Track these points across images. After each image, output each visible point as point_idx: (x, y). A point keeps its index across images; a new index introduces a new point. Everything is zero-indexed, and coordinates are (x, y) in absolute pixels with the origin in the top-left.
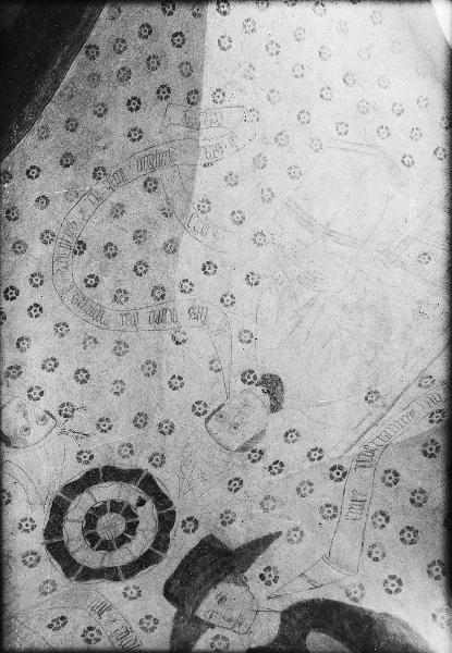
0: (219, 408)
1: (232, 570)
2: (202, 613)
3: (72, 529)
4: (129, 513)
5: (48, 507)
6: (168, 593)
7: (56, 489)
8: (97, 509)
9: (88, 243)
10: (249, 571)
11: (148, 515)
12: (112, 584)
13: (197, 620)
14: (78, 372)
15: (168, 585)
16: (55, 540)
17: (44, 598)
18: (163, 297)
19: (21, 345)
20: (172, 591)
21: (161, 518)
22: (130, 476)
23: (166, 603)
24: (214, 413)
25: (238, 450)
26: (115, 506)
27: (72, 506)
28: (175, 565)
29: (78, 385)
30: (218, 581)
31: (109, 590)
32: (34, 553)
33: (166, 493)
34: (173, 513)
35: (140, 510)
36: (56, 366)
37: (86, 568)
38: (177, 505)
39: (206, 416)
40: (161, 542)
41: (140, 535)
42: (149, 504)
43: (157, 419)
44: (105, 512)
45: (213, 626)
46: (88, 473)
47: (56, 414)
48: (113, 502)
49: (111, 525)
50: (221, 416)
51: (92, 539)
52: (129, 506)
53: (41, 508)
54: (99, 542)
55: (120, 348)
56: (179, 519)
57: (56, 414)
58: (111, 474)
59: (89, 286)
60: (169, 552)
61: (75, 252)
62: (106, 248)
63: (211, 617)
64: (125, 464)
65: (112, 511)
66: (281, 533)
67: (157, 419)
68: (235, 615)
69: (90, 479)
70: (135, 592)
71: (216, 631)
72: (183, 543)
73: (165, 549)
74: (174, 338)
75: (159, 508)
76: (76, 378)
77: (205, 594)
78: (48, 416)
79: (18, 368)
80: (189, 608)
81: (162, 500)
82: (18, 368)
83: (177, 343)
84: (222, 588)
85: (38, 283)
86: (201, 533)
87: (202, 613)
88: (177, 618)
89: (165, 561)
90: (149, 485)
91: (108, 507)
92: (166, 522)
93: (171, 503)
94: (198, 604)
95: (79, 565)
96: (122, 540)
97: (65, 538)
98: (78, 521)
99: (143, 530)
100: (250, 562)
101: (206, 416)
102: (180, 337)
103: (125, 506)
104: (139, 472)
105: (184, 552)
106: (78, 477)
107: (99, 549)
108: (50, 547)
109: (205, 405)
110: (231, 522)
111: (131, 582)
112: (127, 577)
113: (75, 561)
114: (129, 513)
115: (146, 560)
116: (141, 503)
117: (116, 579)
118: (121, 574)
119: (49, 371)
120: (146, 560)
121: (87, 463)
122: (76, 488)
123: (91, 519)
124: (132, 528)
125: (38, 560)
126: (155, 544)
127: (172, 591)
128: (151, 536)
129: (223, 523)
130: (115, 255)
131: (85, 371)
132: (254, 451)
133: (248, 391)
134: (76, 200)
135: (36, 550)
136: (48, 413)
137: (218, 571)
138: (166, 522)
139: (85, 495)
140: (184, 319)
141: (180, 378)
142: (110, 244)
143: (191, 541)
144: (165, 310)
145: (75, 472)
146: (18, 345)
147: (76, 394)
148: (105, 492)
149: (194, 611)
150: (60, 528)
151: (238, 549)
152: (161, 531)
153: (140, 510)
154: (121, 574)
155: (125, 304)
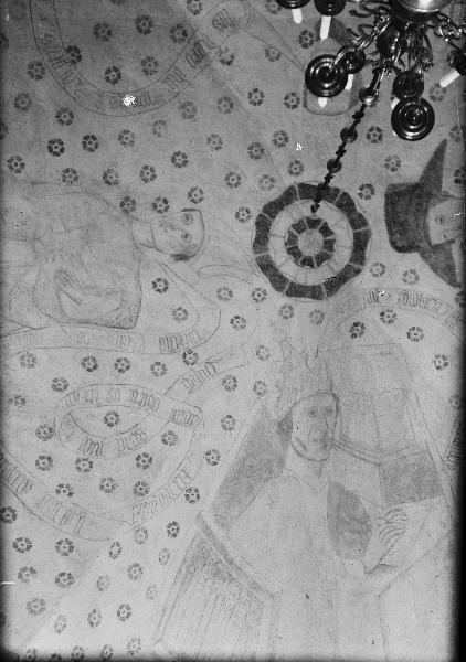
1: (429, 195)
3: (290, 269)
7: (252, 256)
8: (289, 240)
9: (76, 42)
10: (443, 185)
12: (360, 276)
13: (437, 248)
15: (393, 243)
16: (287, 287)
17: (324, 324)
18: (185, 34)
19: (111, 180)
20: (399, 244)
21: (340, 206)
22: (288, 197)
23: (407, 255)
26: (299, 227)
27: (272, 255)
28: (383, 227)
29: (184, 169)
30: (426, 211)
31: (364, 282)
32: (284, 307)
34: (345, 194)
35: (319, 214)
36: (152, 170)
39: (301, 101)
40: (357, 222)
41: (336, 230)
43: (267, 139)
44: (296, 237)
46: (257, 224)
47: (193, 206)
48: (294, 226)
49: (310, 243)
52: (308, 219)
53: (254, 276)
54: (314, 261)
55: (188, 110)
56: (354, 194)
57: (193, 206)
58: (273, 208)
59: (115, 82)
60: (370, 223)
61: (73, 62)
62: (96, 33)
64: (274, 194)
66: (445, 141)
67: (267, 139)
70: (379, 268)
72: (373, 209)
73: (365, 223)
74: (223, 61)
77: (426, 228)
79: (127, 199)
82: (127, 199)
83: (229, 63)
85: (68, 118)
86: (381, 191)
89: (373, 231)
91: (295, 233)
92: (346, 205)
94: (427, 236)
95: (319, 286)
96: (329, 245)
97: (291, 279)
98: (287, 260)
99: (336, 225)
100: (439, 178)
101: (301, 101)
102: (227, 57)
104: (291, 188)
106: (255, 233)
108: (289, 294)
109: (293, 94)
110: (398, 164)
111: (369, 264)
113: (313, 287)
114: (313, 223)
115: (360, 244)
117: (358, 272)
118: (356, 266)
119: (152, 179)
120: (360, 244)
121: (249, 217)
123: (294, 251)
124: (326, 230)
125: (291, 308)
126: (353, 224)
128: (345, 223)
129: (393, 170)
130: (110, 33)
131: (177, 154)
133: (433, 98)
134: (28, 12)
136: (185, 210)
137: (420, 204)
139: (272, 240)
140: (217, 38)
141: (256, 90)
142: (97, 27)
144: (197, 44)
145: (248, 232)
146: (107, 182)
147: (163, 167)
148: (282, 224)
149: (429, 244)
150: (281, 276)
151: (422, 178)
152: (349, 215)
153: (319, 214)
154: (356, 266)
155: (159, 69)
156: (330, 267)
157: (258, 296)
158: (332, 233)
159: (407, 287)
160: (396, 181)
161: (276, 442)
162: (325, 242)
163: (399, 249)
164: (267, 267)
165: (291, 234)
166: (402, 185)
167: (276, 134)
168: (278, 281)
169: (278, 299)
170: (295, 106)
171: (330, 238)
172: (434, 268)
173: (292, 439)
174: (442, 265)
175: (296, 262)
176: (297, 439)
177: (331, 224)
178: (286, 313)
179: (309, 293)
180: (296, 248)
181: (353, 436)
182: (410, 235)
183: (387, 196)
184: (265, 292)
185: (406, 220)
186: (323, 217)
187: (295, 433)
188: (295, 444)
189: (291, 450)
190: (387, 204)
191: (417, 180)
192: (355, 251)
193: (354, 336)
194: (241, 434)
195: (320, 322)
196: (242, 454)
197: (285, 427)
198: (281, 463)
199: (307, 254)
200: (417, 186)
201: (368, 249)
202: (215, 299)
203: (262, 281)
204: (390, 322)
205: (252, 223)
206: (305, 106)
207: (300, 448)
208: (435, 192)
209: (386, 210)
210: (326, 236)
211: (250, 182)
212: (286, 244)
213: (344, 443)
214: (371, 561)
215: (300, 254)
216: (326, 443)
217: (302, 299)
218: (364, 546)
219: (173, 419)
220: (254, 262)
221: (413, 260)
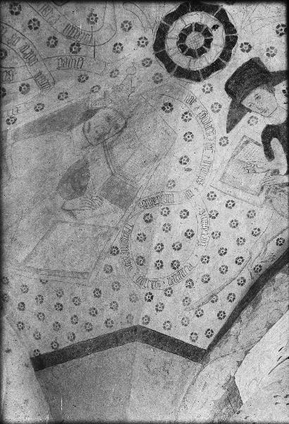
1: (267, 82)
2: (246, 103)
3: (171, 44)
4: (207, 33)
5: (155, 30)
6: (229, 89)
11: (219, 37)
15: (228, 83)
20: (229, 86)
21: (227, 39)
26: (198, 27)
27: (171, 29)
30: (257, 86)
31: (196, 88)
33: (233, 23)
34: (236, 37)
37: (179, 67)
38: (239, 33)
40: (226, 55)
41: (213, 48)
42: (221, 29)
44: (192, 31)
45: (250, 111)
48: (196, 24)
49: (194, 41)
51: (183, 48)
52: (207, 28)
56: (239, 42)
63: (250, 106)
68: (264, 107)
71: (252, 114)
72: (240, 58)
73: (228, 60)
77: (248, 93)
80: (239, 99)
84: (258, 91)
86: (252, 54)
87: (246, 103)
92: (231, 42)
94: (244, 97)
103: (205, 28)
105: (240, 64)
107: (187, 55)
111: (206, 81)
112: (205, 78)
113: (172, 62)
114: (207, 33)
115: (217, 66)
116: (215, 27)
117: (199, 80)
120: (217, 66)
123: (183, 37)
125: (151, 62)
127: (229, 86)
128: (220, 50)
129: (268, 55)
137: (259, 80)
138: (231, 42)
139: (179, 21)
151: (274, 72)
153: (214, 32)
156: (190, 61)
157: (142, 42)
158: (209, 47)
159: (210, 110)
160: (263, 60)
161: (77, 118)
162: (202, 48)
163: (227, 89)
165: (191, 26)
166: (263, 64)
168: (159, 45)
169: (149, 52)
171: (206, 49)
173: (87, 122)
175: (177, 43)
176: (90, 124)
177: (214, 42)
178: (146, 63)
179: (167, 63)
181: (116, 150)
184: (147, 43)
186: (214, 35)
187: (92, 120)
189: (83, 124)
191: (271, 71)
192: (208, 67)
193: (163, 108)
194: (63, 104)
195: (157, 82)
196: (56, 113)
197: (90, 113)
198: (71, 128)
199: (187, 44)
200: (267, 72)
201: (215, 73)
202: (119, 25)
203: (151, 37)
204: (185, 120)
207: (86, 128)
208: (270, 84)
209: (243, 65)
210: (205, 45)
213: (108, 148)
214: (68, 206)
215: (184, 41)
216: (100, 138)
217: (161, 63)
218: (72, 197)
220: (158, 25)
221: (226, 101)
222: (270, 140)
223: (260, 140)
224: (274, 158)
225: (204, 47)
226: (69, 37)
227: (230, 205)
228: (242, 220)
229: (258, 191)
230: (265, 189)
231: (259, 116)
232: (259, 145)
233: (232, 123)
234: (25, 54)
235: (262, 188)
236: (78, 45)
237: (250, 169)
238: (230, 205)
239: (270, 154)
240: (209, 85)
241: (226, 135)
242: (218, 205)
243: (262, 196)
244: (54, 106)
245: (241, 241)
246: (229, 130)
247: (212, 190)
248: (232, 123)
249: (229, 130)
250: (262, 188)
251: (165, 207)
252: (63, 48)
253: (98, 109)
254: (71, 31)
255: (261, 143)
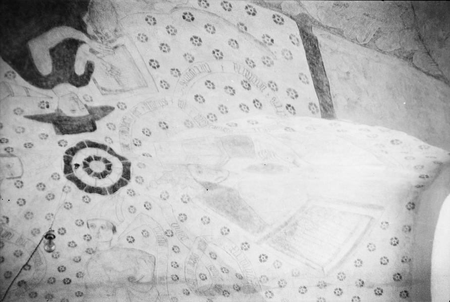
0: (10, 178)
1: (59, 117)
4: (86, 165)
5: (117, 193)
6: (94, 128)
14: (63, 234)
16: (124, 179)
20: (92, 128)
21: (73, 154)
24: (13, 178)
25: (15, 156)
26: (90, 172)
29: (66, 229)
32: (137, 181)
34: (66, 153)
35: (80, 162)
39: (18, 179)
40: (82, 146)
42: (74, 162)
45: (86, 106)
47: (85, 224)
50: (12, 175)
51: (109, 167)
53: (120, 194)
57: (85, 224)
58: (80, 185)
64: (73, 186)
65: (92, 171)
69: (91, 190)
72: (72, 140)
75: (71, 159)
76: (65, 232)
78: (89, 226)
80: (90, 118)
81: (67, 161)
84: (70, 114)
86: (61, 137)
88: (98, 119)
90: (68, 169)
92: (73, 151)
93: (64, 157)
94: (88, 116)
100: (47, 116)
103: (85, 169)
107: (109, 162)
109: (15, 184)
113: (123, 165)
114: (86, 165)
116: (77, 165)
118: (108, 149)
121: (88, 197)
122: (100, 191)
123: (103, 175)
124: (89, 159)
132: (9, 152)
135: (135, 182)
136: (88, 227)
137: (66, 120)
143: (67, 137)
145: (95, 197)
146: (80, 260)
150: (119, 182)
151: (49, 122)
153: (80, 162)
154: (108, 149)
160: (54, 133)
161: (216, 192)
164: (114, 189)
166: (55, 129)
167: (39, 189)
169: (132, 184)
170: (22, 182)
172: (104, 115)
173: (216, 182)
174: (101, 112)
175: (110, 174)
176: (216, 180)
179: (127, 167)
180: (101, 174)
182: (85, 123)
183: (63, 134)
184: (129, 190)
185: (77, 125)
188: (219, 181)
190: (68, 134)
194: (211, 213)
197: (208, 187)
198: (230, 190)
203: (122, 191)
205: (91, 195)
206: (20, 177)
208: (57, 115)
209: (71, 134)
210: (92, 160)
211: (69, 198)
212: (100, 179)
219: (203, 251)
220: (113, 195)
222: (82, 76)
223: (91, 82)
224: (88, 62)
225: (94, 159)
226: (166, 241)
227: (154, 64)
228: (155, 44)
229: (120, 49)
230: (114, 44)
231: (81, 98)
232: (94, 80)
233: (106, 110)
234: (194, 263)
235: (116, 47)
236: (166, 233)
237: (112, 71)
238: (154, 64)
239: (90, 68)
240: (106, 141)
241: (116, 108)
242: (163, 74)
243: (119, 41)
244: (220, 220)
245: (171, 31)
246: (112, 109)
247: (160, 89)
248: (106, 110)
249: (112, 109)
250: (116, 47)
251: (208, 120)
252: (173, 241)
253: (200, 183)
254: (161, 242)
255: (91, 80)
